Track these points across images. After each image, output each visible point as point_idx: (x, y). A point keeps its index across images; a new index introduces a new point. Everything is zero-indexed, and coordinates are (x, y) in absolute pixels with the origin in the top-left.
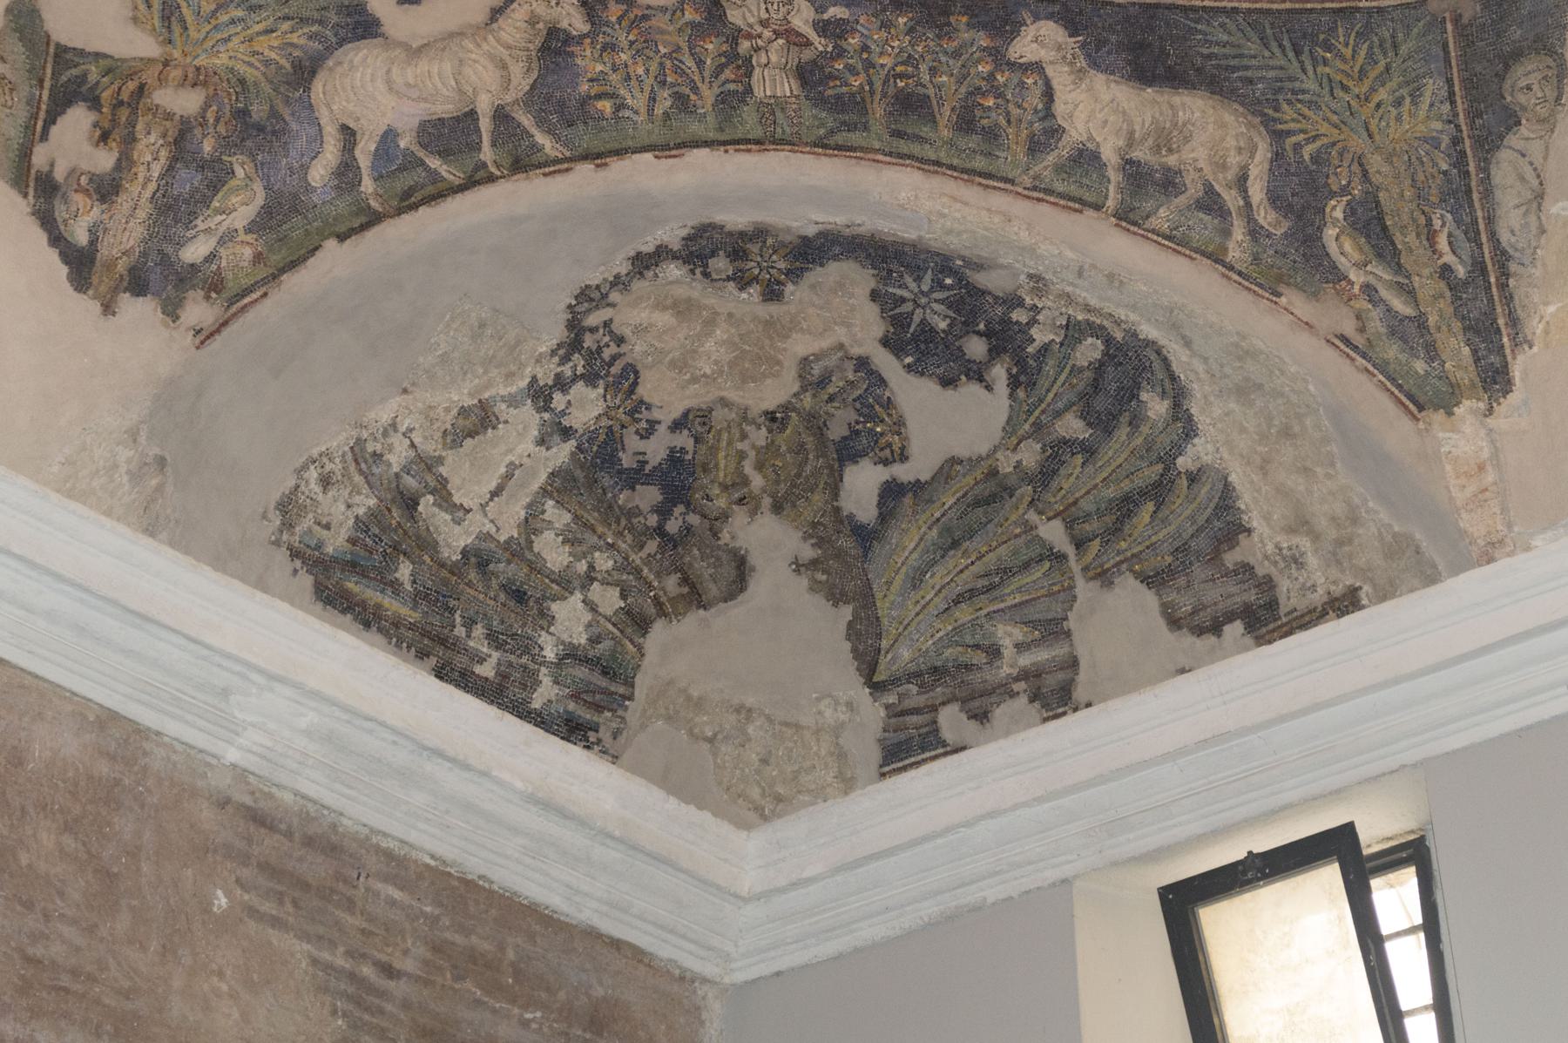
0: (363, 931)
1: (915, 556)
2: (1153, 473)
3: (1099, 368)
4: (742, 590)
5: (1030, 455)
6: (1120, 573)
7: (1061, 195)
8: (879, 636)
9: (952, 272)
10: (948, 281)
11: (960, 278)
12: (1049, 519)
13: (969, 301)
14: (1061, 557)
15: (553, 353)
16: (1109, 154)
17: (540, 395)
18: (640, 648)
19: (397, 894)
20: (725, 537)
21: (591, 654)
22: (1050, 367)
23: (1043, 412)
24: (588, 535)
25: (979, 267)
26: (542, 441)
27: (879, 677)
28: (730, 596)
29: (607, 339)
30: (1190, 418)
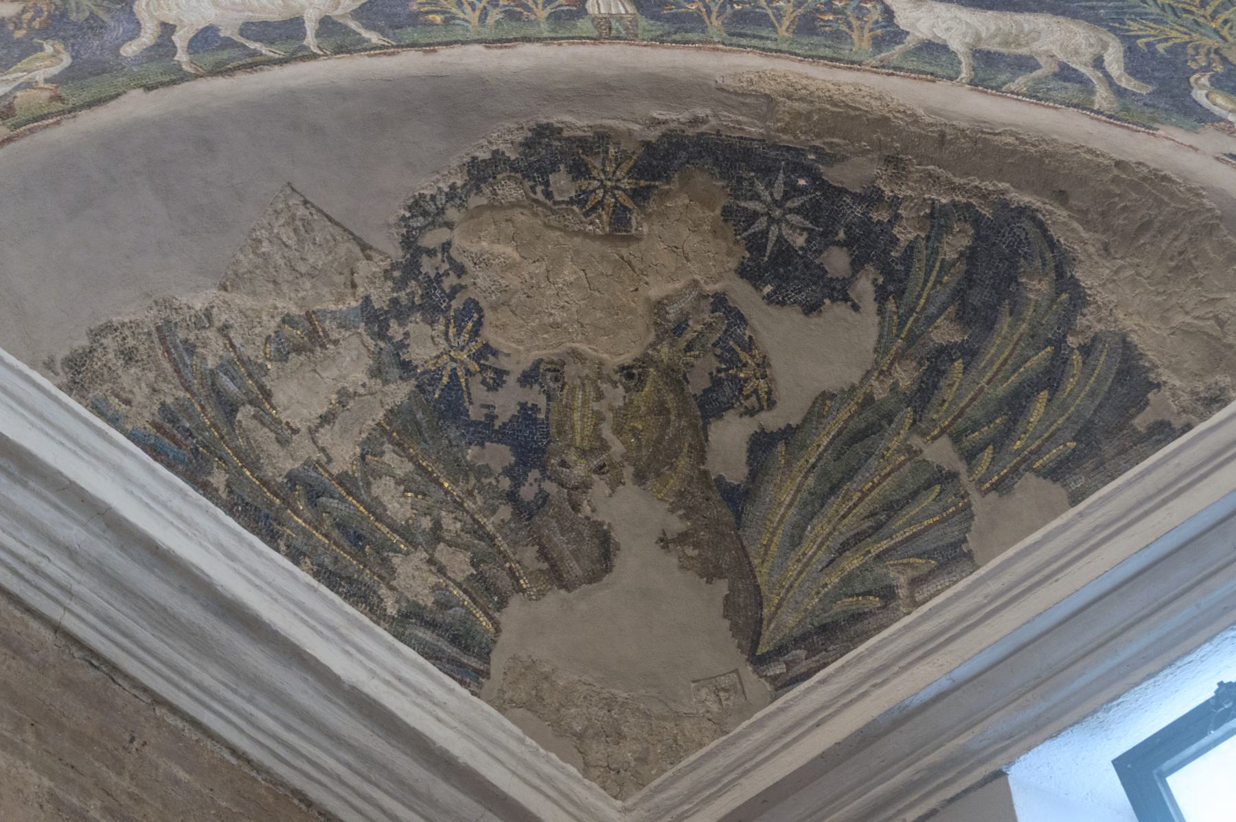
0: (131, 796)
1: (793, 510)
3: (970, 256)
4: (608, 570)
6: (1020, 476)
7: (908, 70)
9: (808, 171)
10: (802, 182)
11: (815, 177)
12: (935, 438)
13: (824, 206)
14: (954, 476)
15: (387, 274)
16: (955, 45)
17: (375, 320)
18: (496, 625)
19: (182, 775)
20: (587, 509)
21: (439, 617)
22: (918, 267)
23: (916, 321)
24: (432, 488)
25: (832, 159)
26: (376, 372)
27: (762, 650)
28: (593, 578)
29: (446, 266)
30: (1075, 283)
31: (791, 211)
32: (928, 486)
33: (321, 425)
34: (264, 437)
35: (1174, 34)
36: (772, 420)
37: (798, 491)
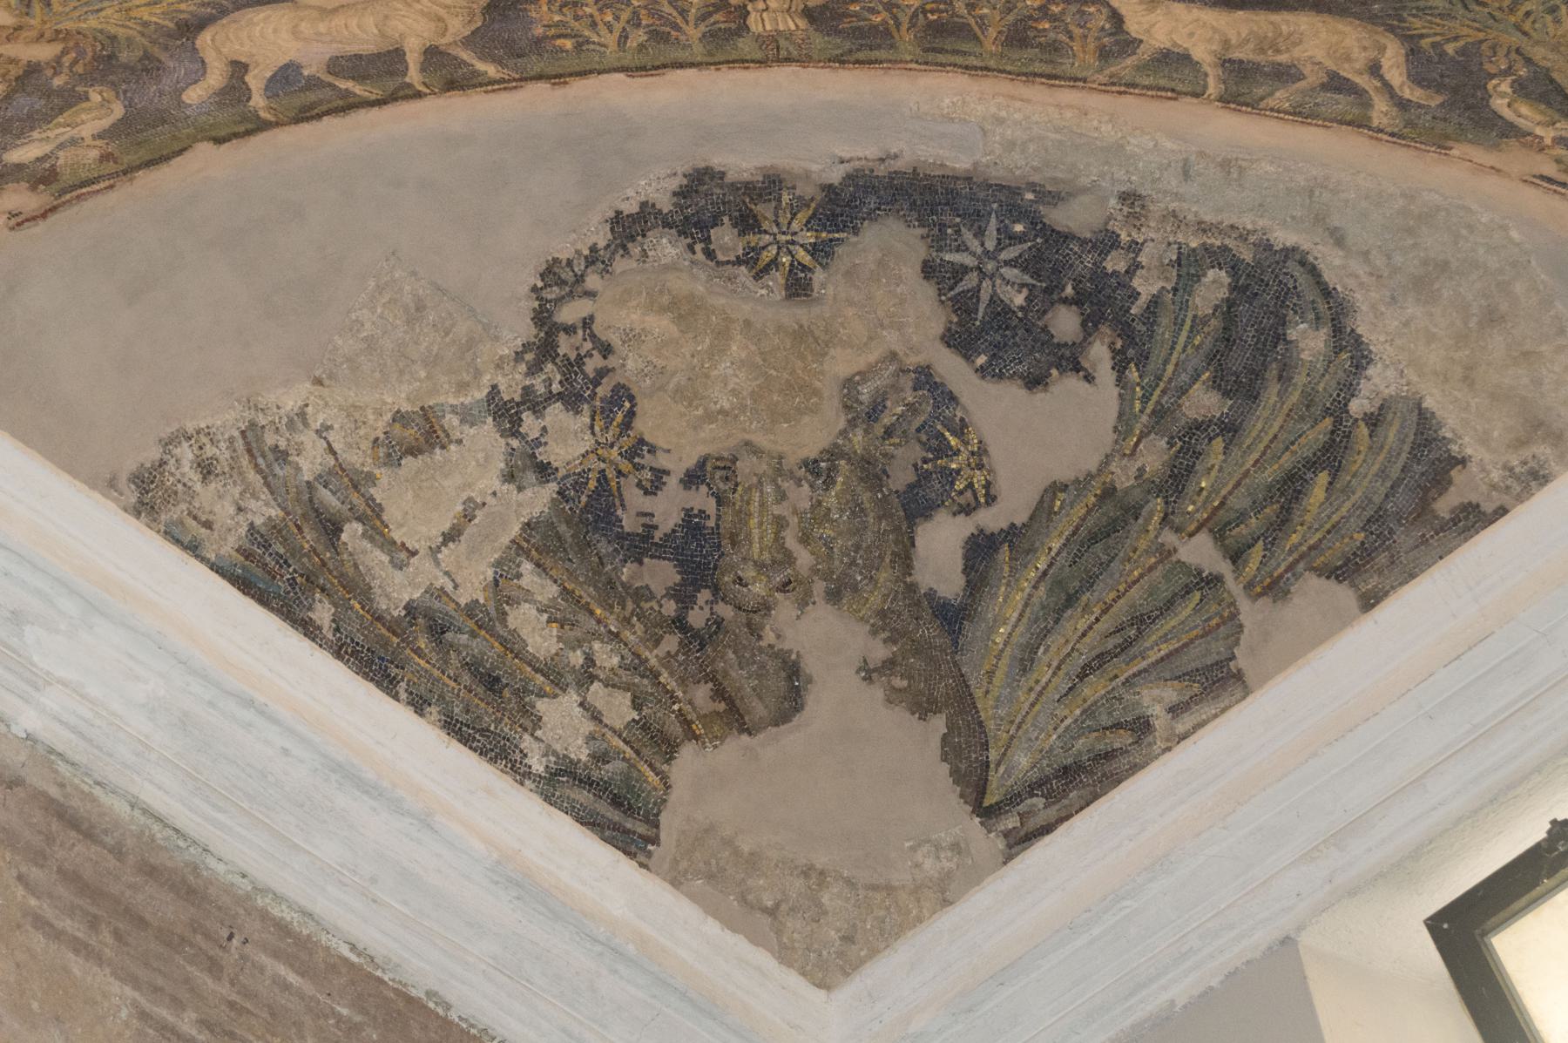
1: (1021, 629)
2: (1316, 435)
3: (1228, 310)
5: (1154, 456)
6: (1297, 577)
7: (1145, 87)
8: (985, 746)
10: (1019, 228)
11: (1035, 222)
12: (1191, 535)
13: (1048, 255)
14: (1215, 580)
15: (518, 357)
16: (1200, 53)
18: (664, 778)
20: (769, 637)
21: (595, 775)
23: (1164, 392)
24: (582, 617)
26: (510, 477)
29: (588, 345)
30: (1358, 341)
31: (1007, 263)
32: (1188, 590)
33: (445, 543)
34: (375, 559)
35: (1466, 31)
36: (992, 519)
37: (1026, 605)
